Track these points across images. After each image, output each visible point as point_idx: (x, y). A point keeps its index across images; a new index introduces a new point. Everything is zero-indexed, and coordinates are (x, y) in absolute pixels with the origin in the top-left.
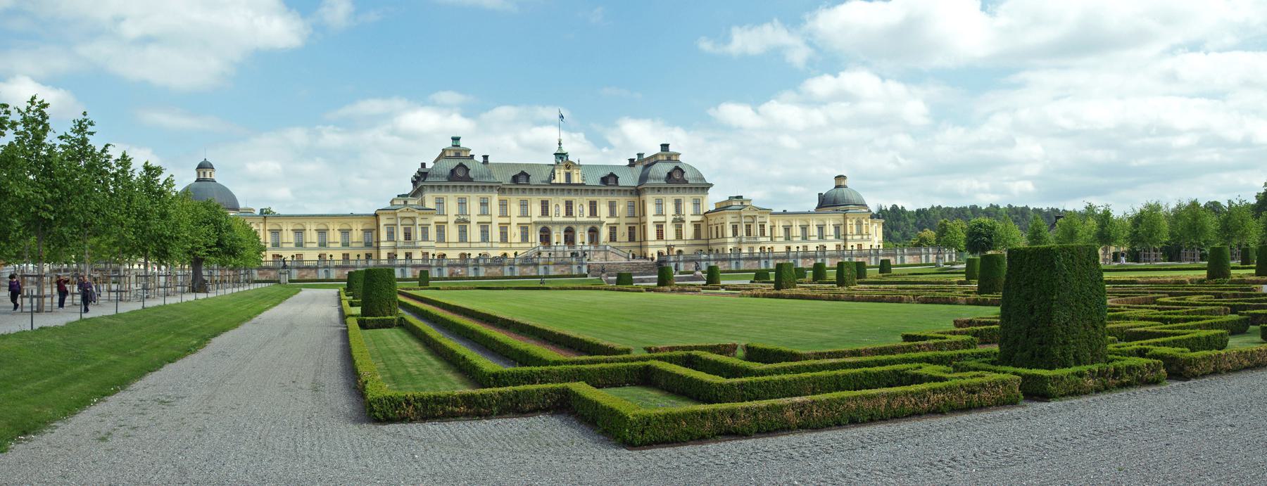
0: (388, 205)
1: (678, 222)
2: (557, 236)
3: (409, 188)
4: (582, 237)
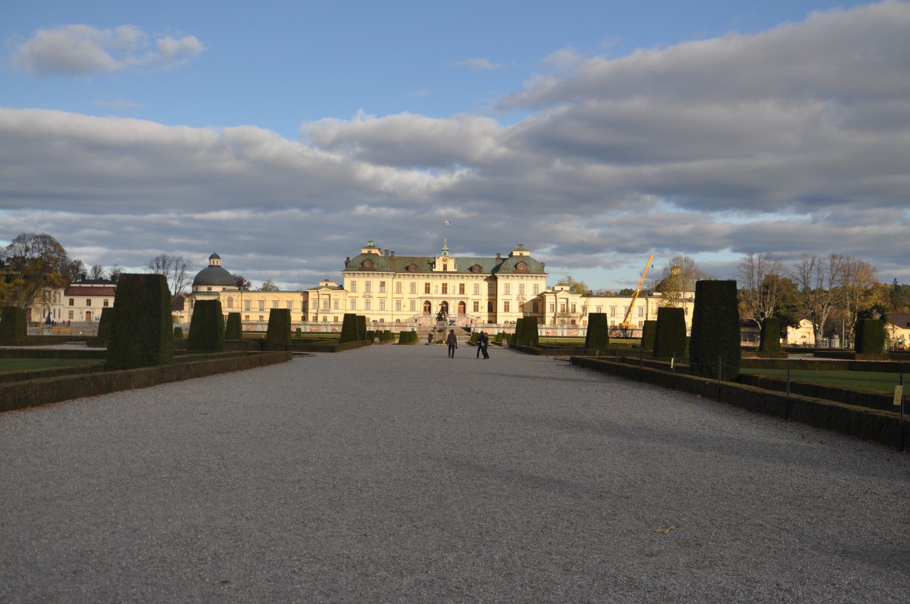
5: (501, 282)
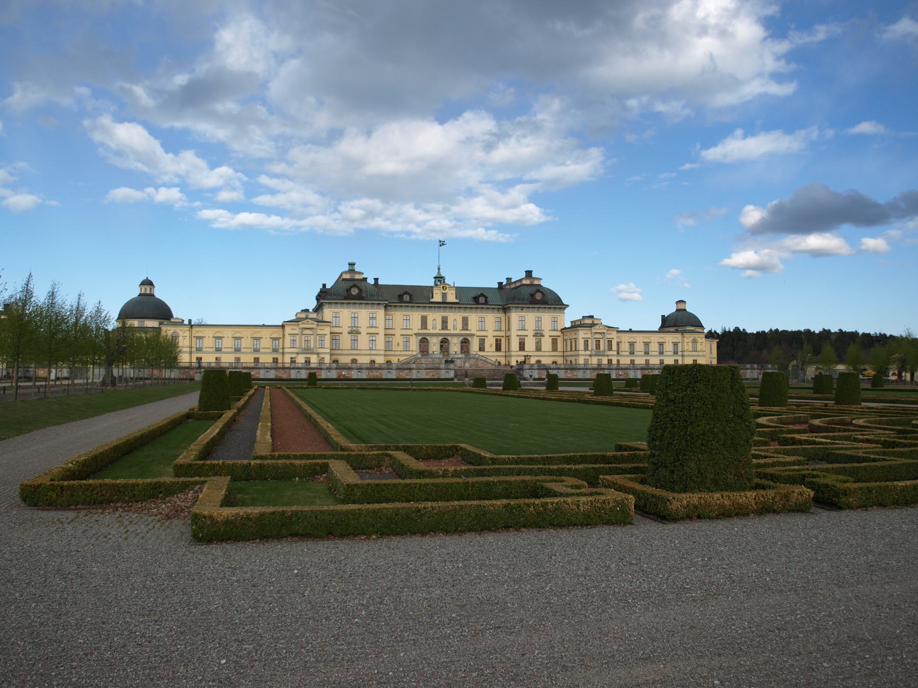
0: (294, 318)
1: (539, 335)
2: (434, 346)
3: (312, 304)
4: (455, 347)
5: (515, 316)
